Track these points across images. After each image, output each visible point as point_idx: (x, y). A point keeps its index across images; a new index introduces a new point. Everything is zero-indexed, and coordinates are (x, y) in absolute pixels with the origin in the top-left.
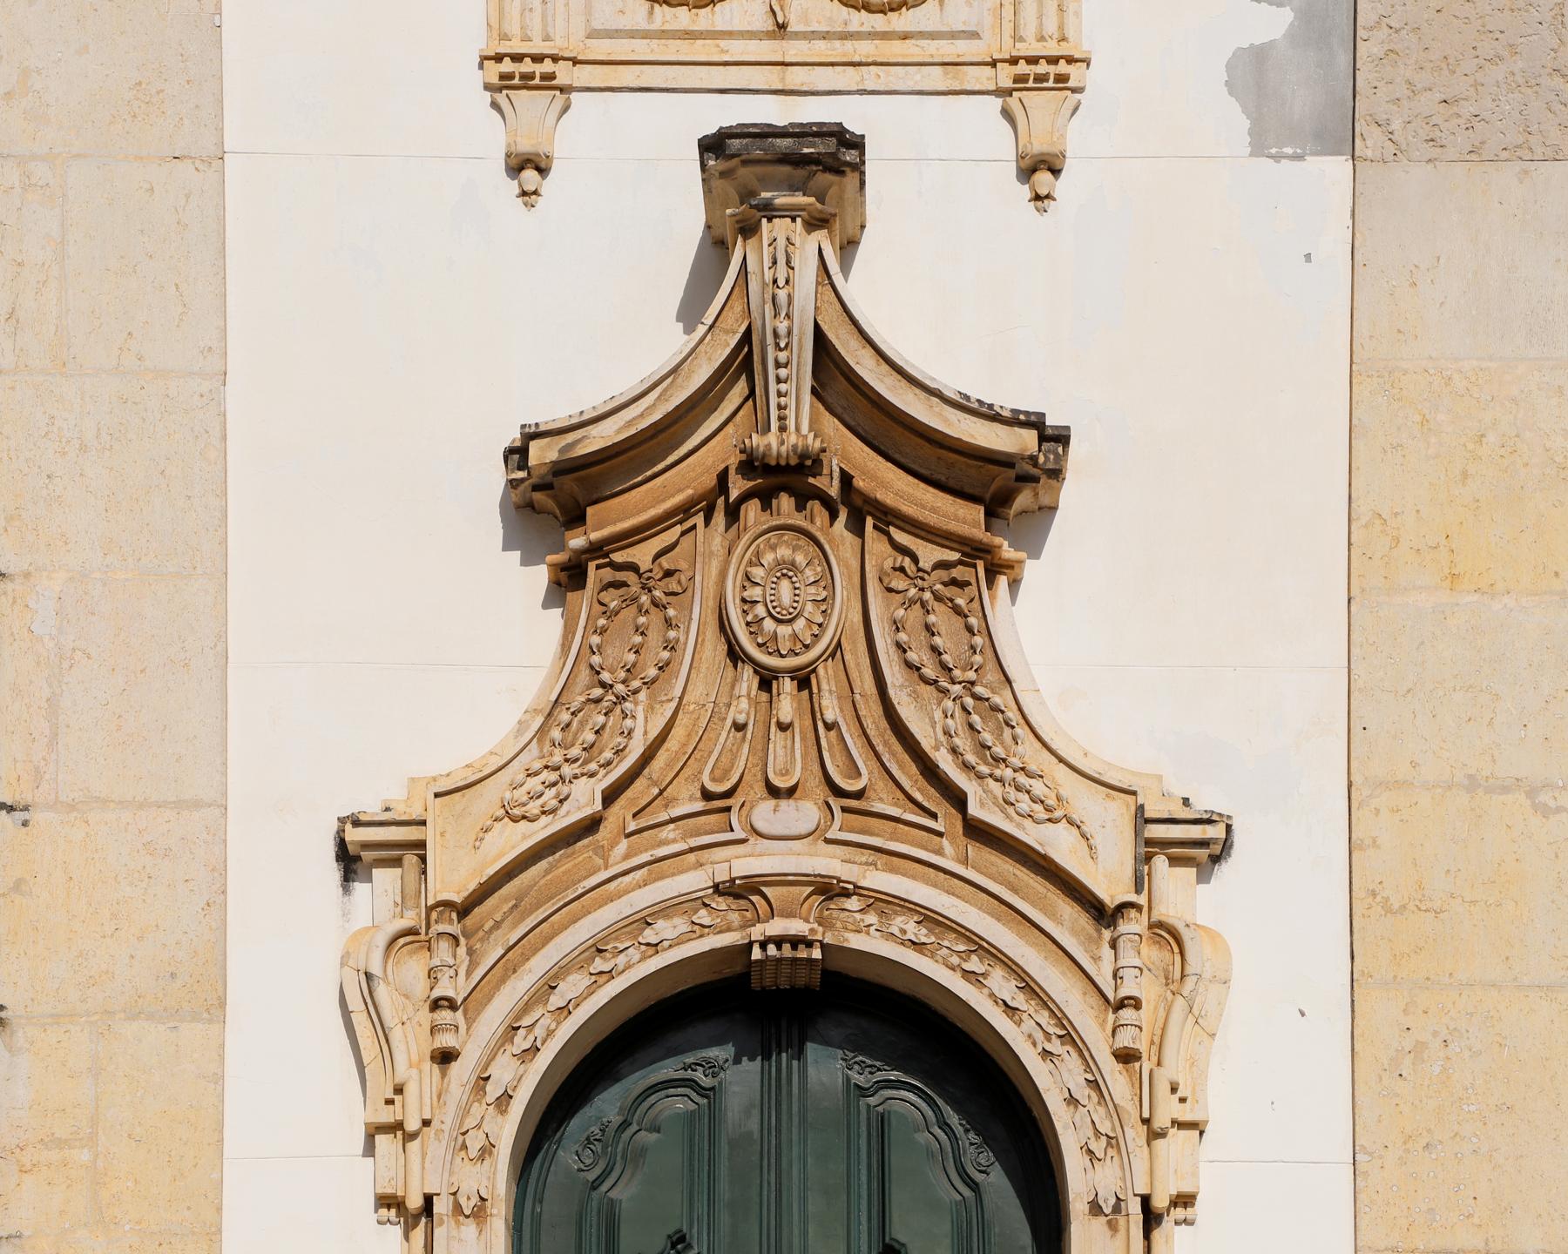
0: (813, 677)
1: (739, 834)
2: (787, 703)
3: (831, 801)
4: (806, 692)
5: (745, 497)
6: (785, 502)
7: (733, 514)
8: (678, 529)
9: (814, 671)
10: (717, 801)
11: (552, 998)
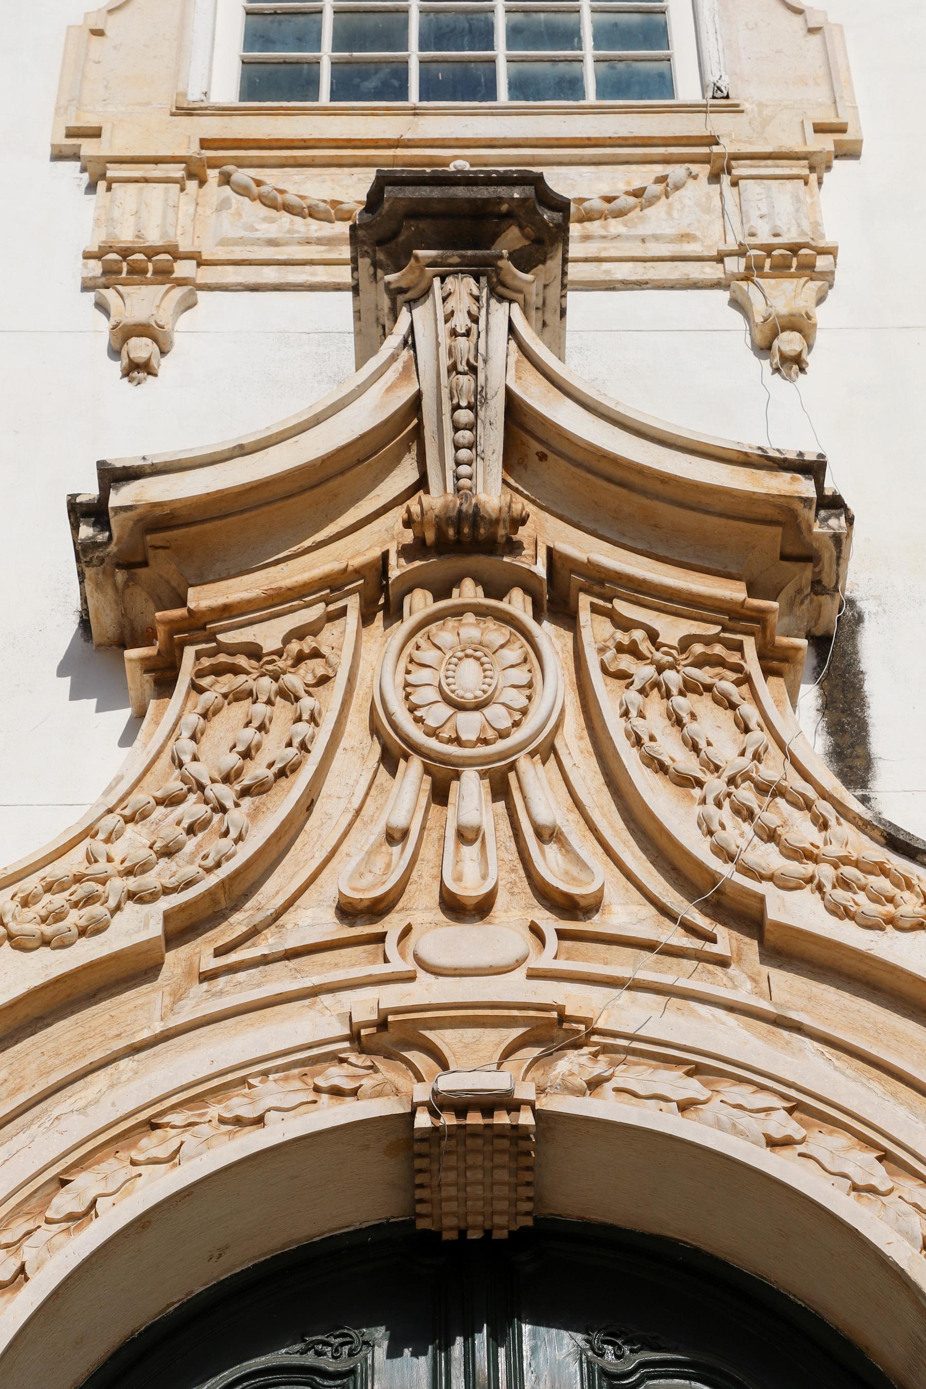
0: (512, 776)
1: (398, 965)
2: (471, 797)
4: (502, 804)
5: (409, 585)
6: (469, 592)
7: (394, 613)
8: (318, 610)
9: (512, 767)
10: (363, 914)
11: (56, 1201)
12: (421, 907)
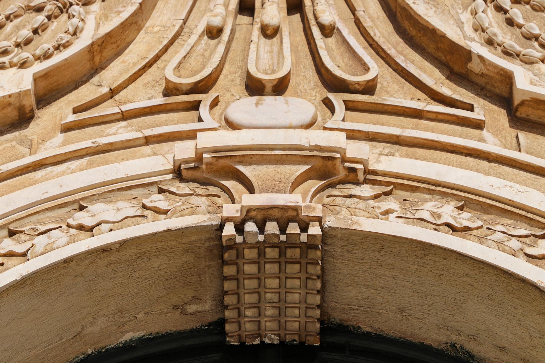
3: (331, 96)
12: (230, 83)
